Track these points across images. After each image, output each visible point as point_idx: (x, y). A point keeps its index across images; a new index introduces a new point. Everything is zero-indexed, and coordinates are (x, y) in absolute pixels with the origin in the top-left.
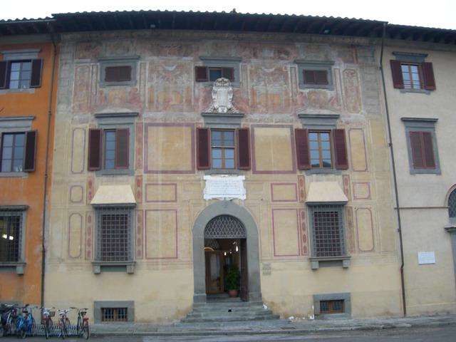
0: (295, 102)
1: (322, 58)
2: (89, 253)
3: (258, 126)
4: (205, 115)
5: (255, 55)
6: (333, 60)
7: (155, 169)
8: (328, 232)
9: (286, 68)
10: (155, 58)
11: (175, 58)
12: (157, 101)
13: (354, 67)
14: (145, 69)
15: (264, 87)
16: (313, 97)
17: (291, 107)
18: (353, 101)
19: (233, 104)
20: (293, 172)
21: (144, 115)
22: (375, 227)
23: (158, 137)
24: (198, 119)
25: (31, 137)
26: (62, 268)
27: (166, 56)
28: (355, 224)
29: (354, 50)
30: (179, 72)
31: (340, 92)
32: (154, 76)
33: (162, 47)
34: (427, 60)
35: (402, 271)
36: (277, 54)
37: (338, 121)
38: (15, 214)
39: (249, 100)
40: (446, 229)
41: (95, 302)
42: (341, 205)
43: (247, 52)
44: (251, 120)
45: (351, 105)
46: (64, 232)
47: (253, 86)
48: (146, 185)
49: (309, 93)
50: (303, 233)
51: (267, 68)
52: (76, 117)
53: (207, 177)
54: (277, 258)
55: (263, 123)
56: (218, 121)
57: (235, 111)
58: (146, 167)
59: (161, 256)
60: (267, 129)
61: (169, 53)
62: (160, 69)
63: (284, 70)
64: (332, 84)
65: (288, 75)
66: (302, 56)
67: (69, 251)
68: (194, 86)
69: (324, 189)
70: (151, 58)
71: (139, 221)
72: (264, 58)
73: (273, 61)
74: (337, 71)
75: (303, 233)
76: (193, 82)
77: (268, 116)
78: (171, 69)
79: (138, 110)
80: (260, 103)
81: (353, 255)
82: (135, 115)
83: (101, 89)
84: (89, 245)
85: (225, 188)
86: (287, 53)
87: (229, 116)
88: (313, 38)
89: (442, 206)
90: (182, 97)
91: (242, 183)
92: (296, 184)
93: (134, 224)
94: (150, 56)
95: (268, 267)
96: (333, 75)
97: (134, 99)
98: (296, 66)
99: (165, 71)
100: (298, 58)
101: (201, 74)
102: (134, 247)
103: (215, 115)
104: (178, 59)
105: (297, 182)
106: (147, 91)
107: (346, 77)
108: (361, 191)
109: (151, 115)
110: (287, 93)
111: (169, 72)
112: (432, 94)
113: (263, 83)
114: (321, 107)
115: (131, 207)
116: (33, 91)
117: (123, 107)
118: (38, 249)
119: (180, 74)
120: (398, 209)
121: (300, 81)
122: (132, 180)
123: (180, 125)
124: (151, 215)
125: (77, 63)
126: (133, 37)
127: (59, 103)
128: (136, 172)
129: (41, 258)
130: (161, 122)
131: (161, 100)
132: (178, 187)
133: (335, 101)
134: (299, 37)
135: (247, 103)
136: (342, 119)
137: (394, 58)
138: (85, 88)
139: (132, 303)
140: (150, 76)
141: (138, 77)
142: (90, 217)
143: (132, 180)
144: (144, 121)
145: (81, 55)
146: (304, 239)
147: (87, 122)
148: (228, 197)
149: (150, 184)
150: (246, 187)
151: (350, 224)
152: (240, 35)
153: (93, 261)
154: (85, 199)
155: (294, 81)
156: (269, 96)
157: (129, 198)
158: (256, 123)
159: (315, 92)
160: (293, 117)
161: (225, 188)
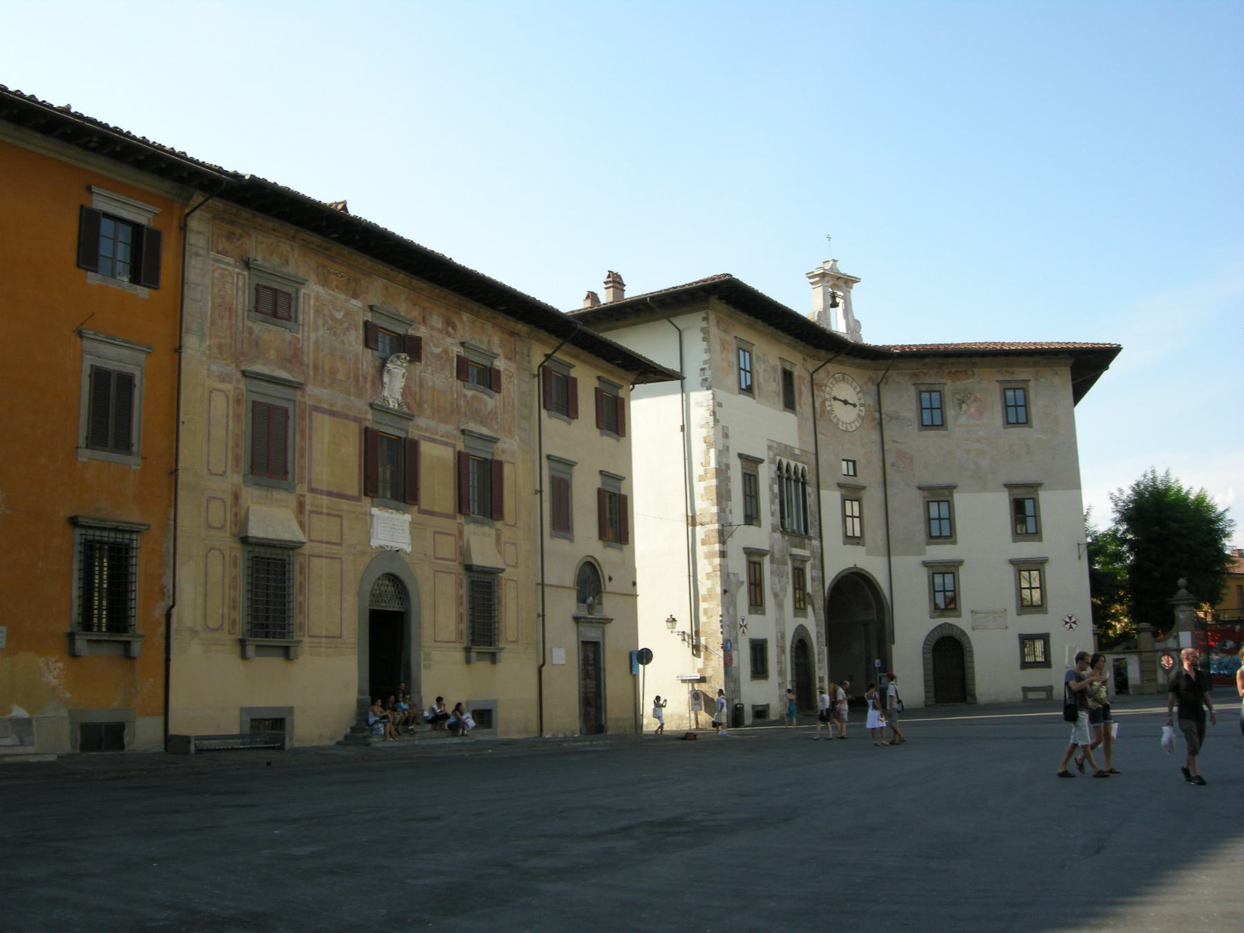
2: (234, 621)
3: (426, 439)
11: (343, 297)
20: (453, 517)
23: (323, 428)
24: (366, 413)
26: (196, 648)
38: (120, 537)
41: (242, 709)
46: (199, 586)
48: (311, 512)
49: (474, 397)
52: (214, 368)
53: (375, 511)
58: (310, 482)
67: (205, 618)
77: (433, 423)
82: (298, 386)
83: (250, 324)
84: (235, 608)
85: (391, 529)
91: (407, 526)
97: (295, 356)
99: (332, 316)
101: (371, 335)
114: (481, 423)
118: (158, 612)
122: (292, 499)
123: (347, 417)
126: (293, 238)
127: (187, 332)
129: (162, 629)
130: (326, 407)
132: (345, 522)
138: (227, 314)
140: (315, 321)
142: (236, 557)
143: (292, 499)
145: (220, 247)
147: (230, 382)
152: (415, 282)
154: (228, 525)
158: (428, 435)
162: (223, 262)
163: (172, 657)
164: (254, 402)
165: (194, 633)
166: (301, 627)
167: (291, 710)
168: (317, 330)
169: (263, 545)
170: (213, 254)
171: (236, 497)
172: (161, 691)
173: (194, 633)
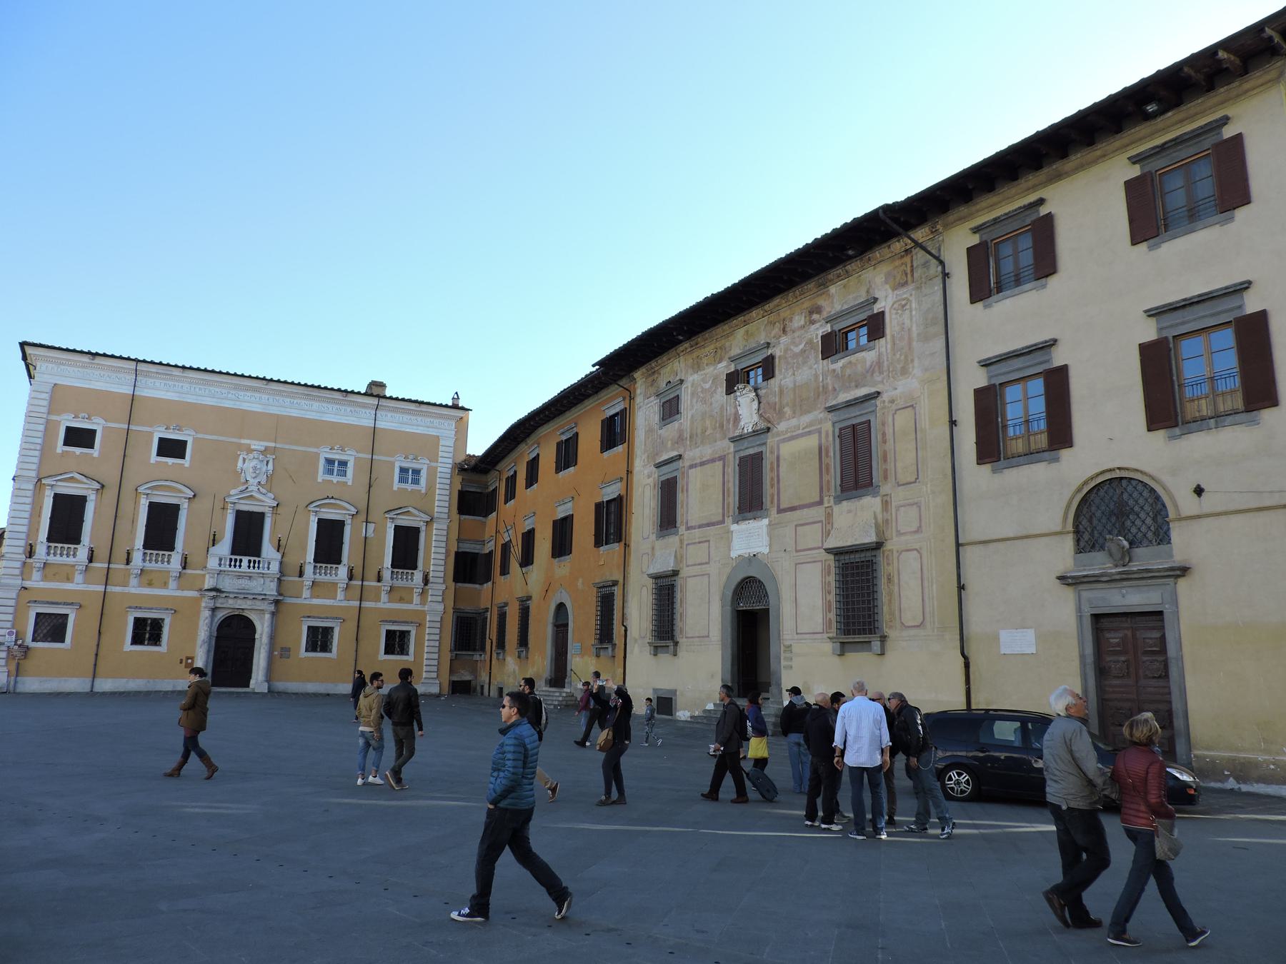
3: (784, 440)
10: (696, 377)
16: (848, 372)
19: (761, 416)
31: (883, 349)
37: (878, 402)
43: (777, 330)
44: (778, 434)
45: (899, 367)
49: (843, 368)
56: (746, 443)
57: (763, 425)
77: (794, 422)
78: (707, 386)
82: (680, 457)
85: (750, 538)
87: (756, 433)
88: (848, 267)
89: (1059, 529)
91: (765, 530)
108: (905, 519)
110: (816, 376)
112: (1053, 281)
115: (675, 573)
120: (958, 545)
124: (691, 582)
131: (699, 431)
134: (830, 277)
136: (885, 397)
144: (687, 464)
152: (766, 307)
165: (636, 641)
173: (636, 641)
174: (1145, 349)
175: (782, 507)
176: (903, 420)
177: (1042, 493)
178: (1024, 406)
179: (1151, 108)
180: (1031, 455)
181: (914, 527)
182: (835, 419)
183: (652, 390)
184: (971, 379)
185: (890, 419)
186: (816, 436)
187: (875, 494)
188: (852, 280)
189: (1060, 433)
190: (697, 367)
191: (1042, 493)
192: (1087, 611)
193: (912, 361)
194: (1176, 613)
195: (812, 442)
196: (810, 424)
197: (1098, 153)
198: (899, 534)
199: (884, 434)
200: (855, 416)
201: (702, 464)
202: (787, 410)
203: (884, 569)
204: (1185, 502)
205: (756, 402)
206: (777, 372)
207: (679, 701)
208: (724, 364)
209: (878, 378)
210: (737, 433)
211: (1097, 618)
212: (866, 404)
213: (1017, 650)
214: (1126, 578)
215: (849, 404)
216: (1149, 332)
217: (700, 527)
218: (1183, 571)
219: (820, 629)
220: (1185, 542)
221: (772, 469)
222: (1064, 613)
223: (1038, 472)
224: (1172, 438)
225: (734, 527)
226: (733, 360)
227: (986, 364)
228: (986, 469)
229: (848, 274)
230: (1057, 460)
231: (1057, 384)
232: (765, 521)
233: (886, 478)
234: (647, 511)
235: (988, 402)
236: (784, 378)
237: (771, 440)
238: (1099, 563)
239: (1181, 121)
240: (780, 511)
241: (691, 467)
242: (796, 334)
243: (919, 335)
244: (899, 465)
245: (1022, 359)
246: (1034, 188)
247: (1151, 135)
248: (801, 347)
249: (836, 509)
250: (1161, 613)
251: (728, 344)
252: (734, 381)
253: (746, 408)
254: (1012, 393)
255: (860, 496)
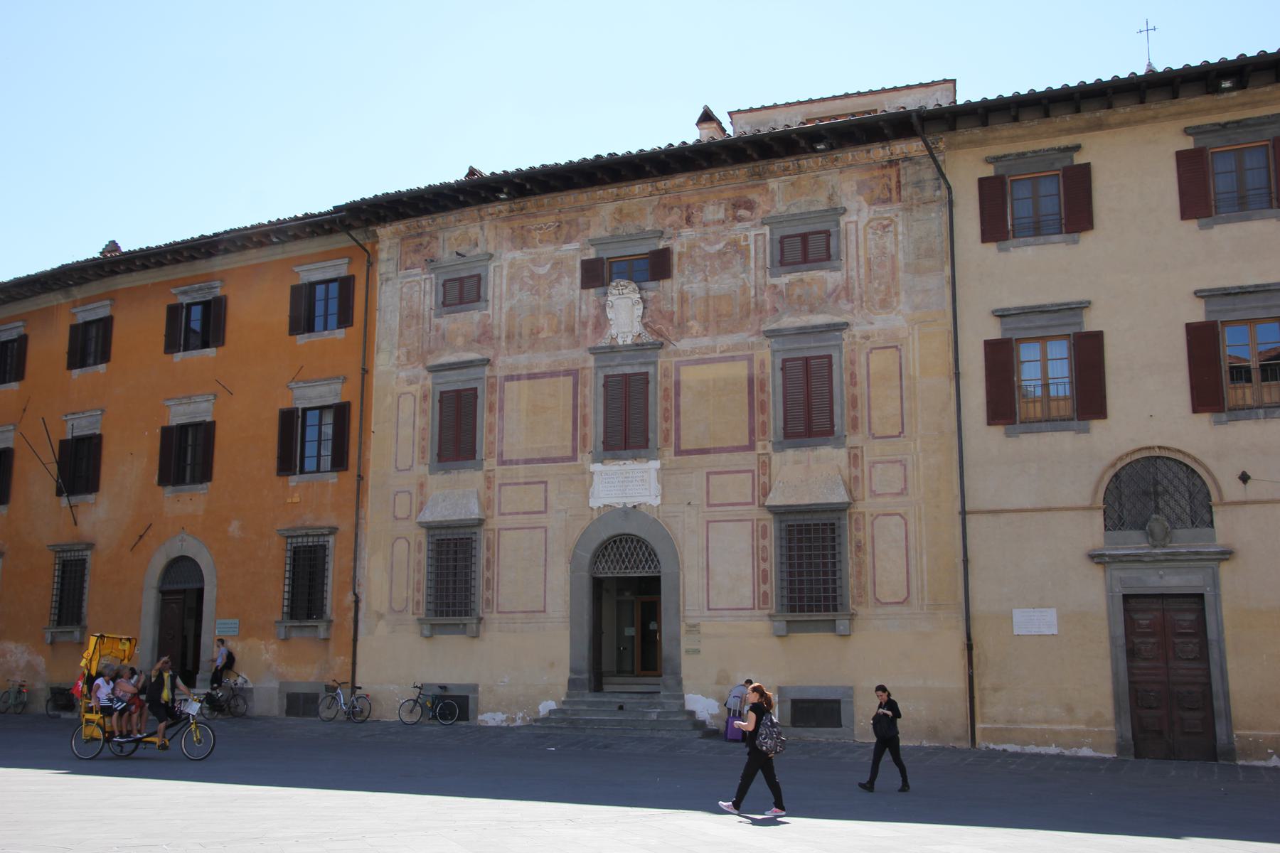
0: (759, 308)
1: (822, 203)
4: (595, 351)
5: (689, 221)
6: (845, 204)
7: (514, 457)
8: (812, 567)
9: (746, 238)
10: (518, 254)
11: (548, 249)
12: (520, 335)
13: (887, 211)
14: (501, 276)
15: (702, 284)
16: (798, 291)
17: (752, 317)
18: (883, 287)
19: (646, 325)
21: (500, 361)
22: (912, 553)
23: (518, 397)
24: (585, 361)
25: (341, 412)
26: (382, 628)
27: (535, 247)
28: (869, 549)
29: (892, 172)
30: (555, 276)
31: (854, 273)
32: (516, 287)
33: (529, 231)
34: (1079, 159)
35: (970, 647)
36: (730, 212)
37: (845, 335)
39: (673, 313)
40: (1096, 558)
42: (839, 509)
43: (675, 216)
44: (677, 353)
45: (877, 298)
46: (386, 572)
47: (683, 284)
48: (501, 485)
49: (789, 285)
50: (762, 566)
51: (711, 244)
52: (403, 374)
54: (712, 613)
55: (697, 356)
57: (648, 338)
58: (501, 455)
59: (521, 609)
60: (705, 367)
61: (541, 241)
62: (526, 273)
63: (743, 243)
64: (839, 258)
65: (749, 250)
66: (781, 208)
67: (391, 602)
68: (581, 299)
69: (807, 477)
70: (509, 256)
71: (488, 549)
72: (705, 225)
73: (722, 228)
74: (852, 226)
75: (762, 566)
76: (578, 292)
77: (705, 341)
78: (542, 271)
79: (488, 353)
80: (695, 318)
81: (861, 611)
82: (486, 362)
83: (435, 321)
84: (418, 590)
85: (626, 485)
86: (750, 206)
87: (638, 347)
88: (804, 163)
89: (1087, 503)
90: (560, 322)
91: (654, 475)
92: (752, 471)
93: (482, 555)
94: (509, 250)
95: (694, 628)
96: (842, 236)
98: (767, 230)
99: (533, 275)
100: (773, 213)
101: (595, 275)
102: (481, 593)
103: (613, 349)
104: (556, 250)
105: (755, 468)
106: (504, 316)
107: (870, 236)
108: (884, 478)
109: (510, 360)
110: (745, 289)
111: (540, 276)
112: (1086, 238)
113: (700, 276)
114: (811, 311)
115: (480, 522)
116: (340, 334)
117: (468, 350)
119: (558, 280)
120: (964, 513)
121: (772, 262)
124: (507, 538)
125: (404, 277)
128: (485, 463)
129: (352, 614)
130: (524, 372)
131: (526, 331)
132: (549, 486)
133: (843, 294)
135: (671, 321)
136: (856, 331)
137: (989, 171)
139: (475, 688)
141: (490, 296)
142: (420, 544)
144: (500, 373)
145: (409, 262)
146: (765, 578)
147: (417, 383)
148: (630, 502)
149: (506, 484)
150: (663, 482)
151: (859, 548)
152: (661, 185)
153: (423, 616)
155: (760, 263)
156: (711, 303)
157: (474, 512)
159: (801, 280)
160: (753, 339)
161: (626, 485)
162: (409, 276)
163: (360, 637)
164: (442, 393)
165: (380, 616)
166: (488, 603)
167: (475, 688)
168: (512, 296)
169: (437, 528)
170: (403, 272)
171: (422, 486)
172: (350, 668)
173: (380, 616)
174: (1191, 329)
175: (683, 447)
176: (881, 361)
177: (1073, 463)
178: (1045, 370)
179: (1226, 84)
180: (1050, 421)
181: (898, 487)
182: (776, 347)
183: (416, 258)
184: (980, 330)
185: (863, 359)
186: (745, 363)
187: (839, 443)
188: (806, 179)
189: (1090, 399)
190: (521, 240)
191: (1073, 463)
192: (1119, 591)
193: (897, 294)
194: (1217, 596)
195: (739, 371)
196: (735, 347)
197: (1151, 113)
198: (874, 494)
199: (853, 376)
200: (810, 348)
201: (532, 377)
202: (695, 326)
203: (850, 535)
204: (1232, 489)
205: (641, 306)
206: (675, 271)
207: (484, 698)
208: (575, 246)
209: (844, 305)
210: (604, 342)
211: (1126, 598)
212: (831, 335)
213: (1034, 631)
214: (1172, 558)
215: (802, 332)
216: (1197, 314)
217: (527, 462)
218: (1226, 555)
219: (749, 603)
220: (1228, 527)
221: (666, 397)
222: (1094, 594)
223: (1064, 442)
224: (1218, 423)
225: (596, 467)
226: (594, 242)
227: (1002, 315)
228: (998, 431)
229: (800, 170)
230: (1087, 431)
231: (1089, 354)
232: (655, 464)
233: (855, 425)
234: (406, 432)
235: (1000, 358)
236: (685, 282)
237: (665, 359)
238: (1133, 542)
239: (1243, 105)
240: (679, 452)
241: (510, 378)
242: (710, 229)
243: (906, 265)
244: (875, 414)
245: (1046, 315)
246: (1069, 131)
247: (1208, 111)
248: (718, 247)
249: (776, 458)
250: (1201, 596)
251: (581, 220)
252: (595, 275)
253: (625, 312)
254: (1028, 353)
255: (816, 445)
